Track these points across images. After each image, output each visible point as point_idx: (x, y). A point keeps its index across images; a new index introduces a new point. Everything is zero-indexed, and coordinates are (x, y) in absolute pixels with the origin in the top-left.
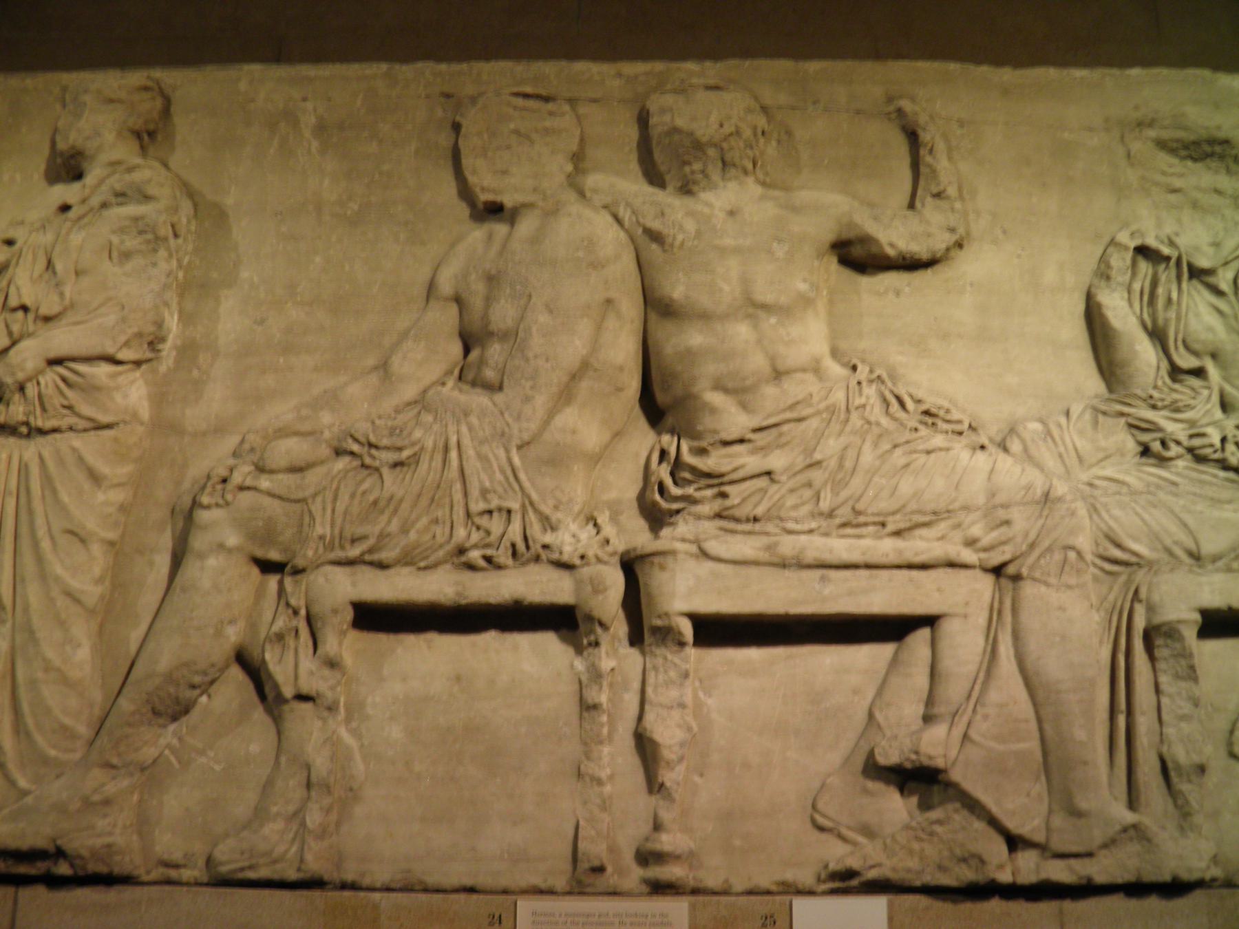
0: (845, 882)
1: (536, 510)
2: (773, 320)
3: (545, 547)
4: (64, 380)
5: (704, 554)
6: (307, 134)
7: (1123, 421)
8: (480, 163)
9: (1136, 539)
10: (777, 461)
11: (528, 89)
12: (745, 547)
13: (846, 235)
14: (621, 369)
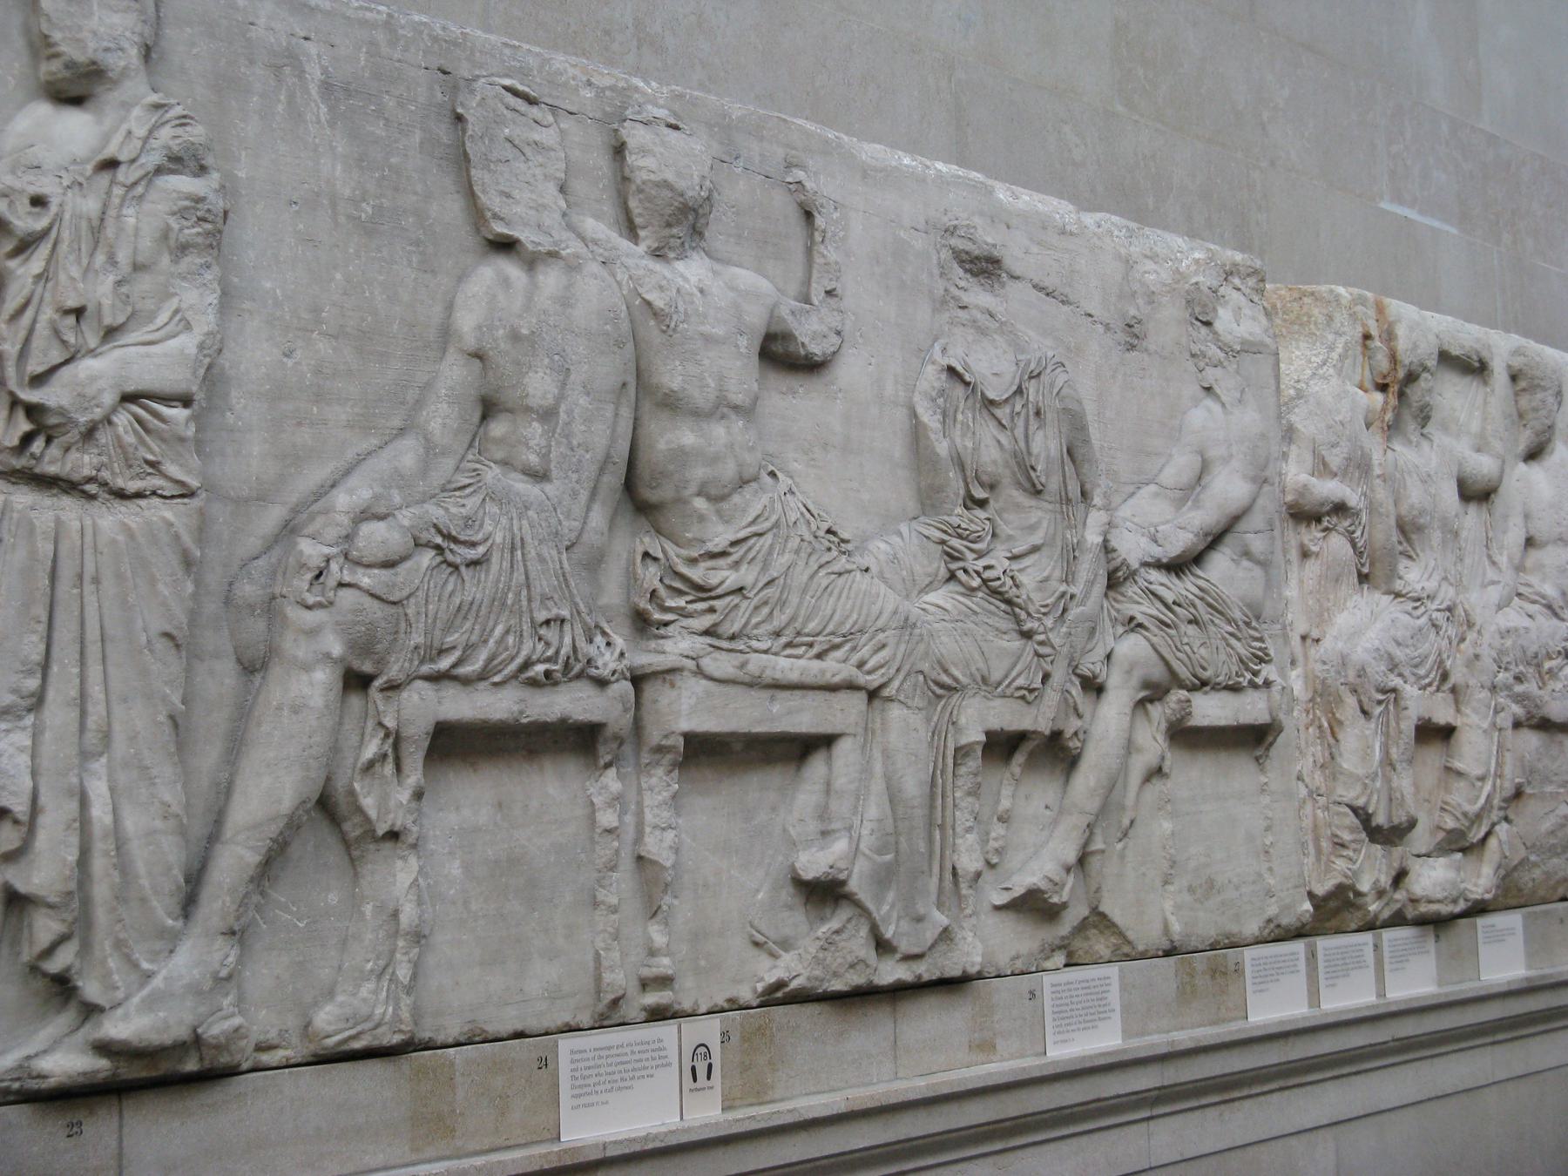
4: (139, 421)
5: (699, 672)
6: (314, 91)
9: (956, 665)
12: (721, 664)
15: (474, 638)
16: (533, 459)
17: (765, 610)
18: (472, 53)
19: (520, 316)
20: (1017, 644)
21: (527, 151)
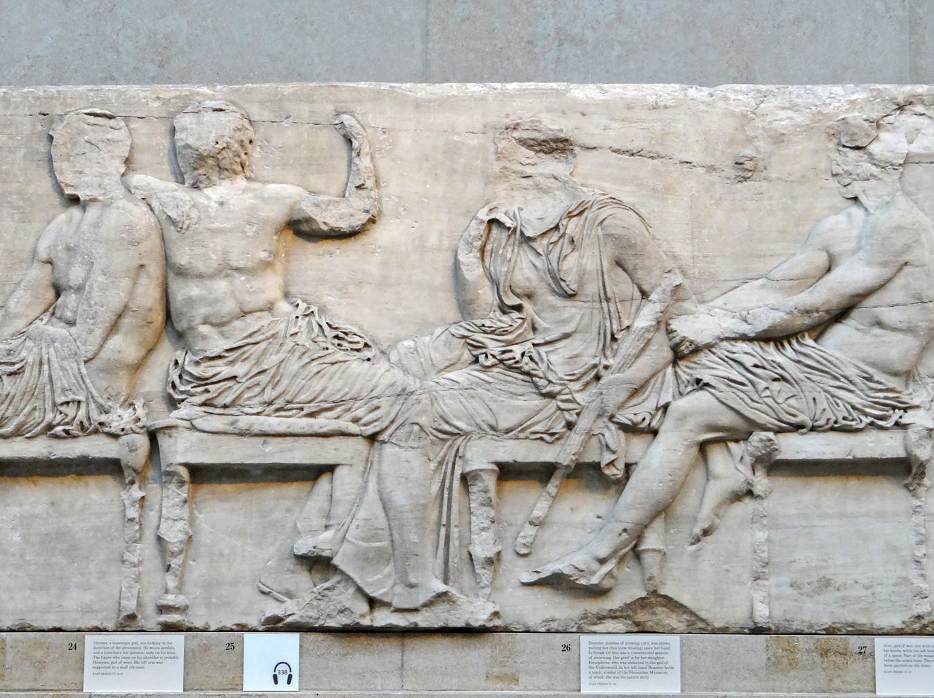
0: (274, 625)
1: (95, 402)
2: (243, 278)
3: (101, 424)
5: (193, 428)
7: (463, 340)
8: (65, 165)
9: (458, 418)
10: (240, 369)
11: (98, 111)
12: (217, 423)
13: (296, 217)
14: (150, 310)
15: (7, 414)
16: (68, 314)
17: (258, 389)
18: (65, 99)
19: (72, 237)
20: (537, 402)
21: (101, 145)
